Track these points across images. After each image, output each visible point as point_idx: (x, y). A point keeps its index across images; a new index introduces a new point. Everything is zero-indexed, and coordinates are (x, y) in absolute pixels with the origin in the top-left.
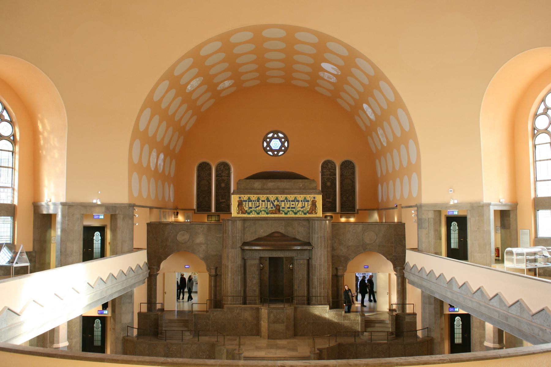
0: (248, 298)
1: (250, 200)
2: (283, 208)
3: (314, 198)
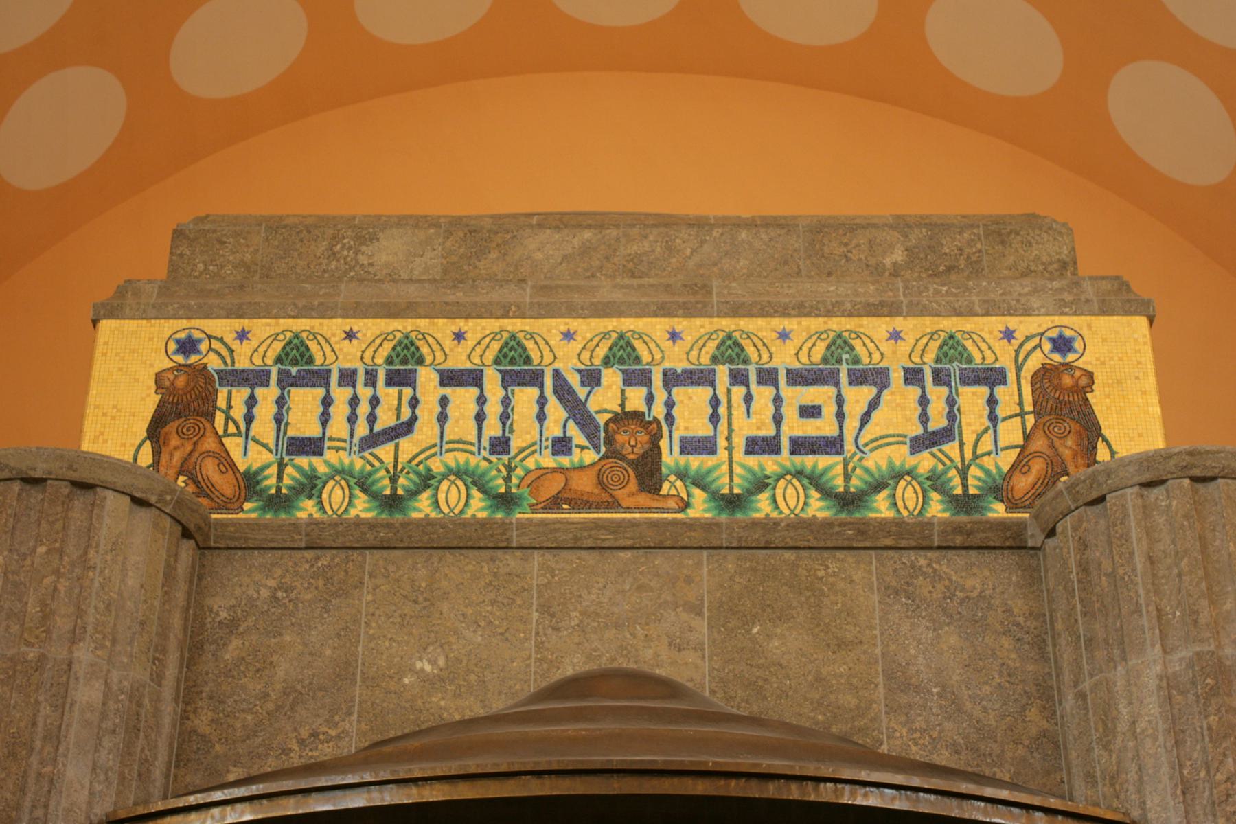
1: (299, 367)
3: (1062, 344)
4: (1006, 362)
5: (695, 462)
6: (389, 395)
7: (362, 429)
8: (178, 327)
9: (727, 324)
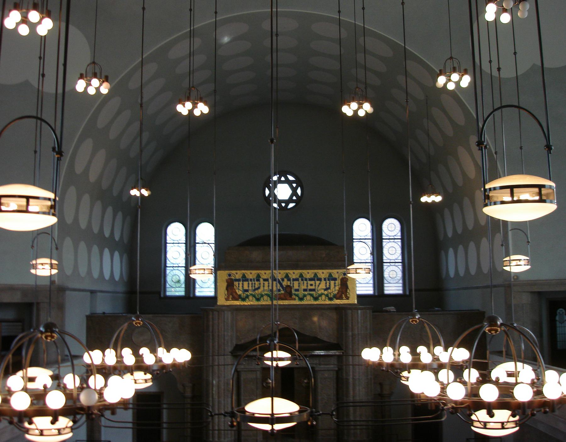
0: (243, 433)
1: (244, 278)
2: (297, 290)
3: (345, 274)
4: (337, 277)
5: (296, 293)
6: (257, 283)
7: (253, 288)
8: (227, 272)
9: (301, 271)
